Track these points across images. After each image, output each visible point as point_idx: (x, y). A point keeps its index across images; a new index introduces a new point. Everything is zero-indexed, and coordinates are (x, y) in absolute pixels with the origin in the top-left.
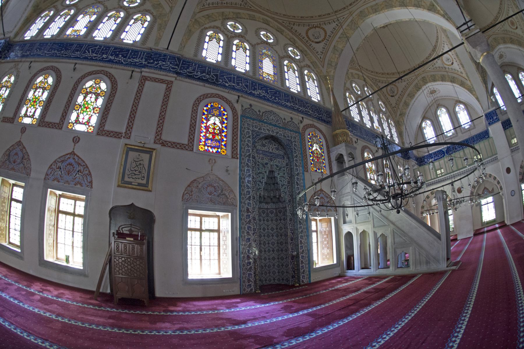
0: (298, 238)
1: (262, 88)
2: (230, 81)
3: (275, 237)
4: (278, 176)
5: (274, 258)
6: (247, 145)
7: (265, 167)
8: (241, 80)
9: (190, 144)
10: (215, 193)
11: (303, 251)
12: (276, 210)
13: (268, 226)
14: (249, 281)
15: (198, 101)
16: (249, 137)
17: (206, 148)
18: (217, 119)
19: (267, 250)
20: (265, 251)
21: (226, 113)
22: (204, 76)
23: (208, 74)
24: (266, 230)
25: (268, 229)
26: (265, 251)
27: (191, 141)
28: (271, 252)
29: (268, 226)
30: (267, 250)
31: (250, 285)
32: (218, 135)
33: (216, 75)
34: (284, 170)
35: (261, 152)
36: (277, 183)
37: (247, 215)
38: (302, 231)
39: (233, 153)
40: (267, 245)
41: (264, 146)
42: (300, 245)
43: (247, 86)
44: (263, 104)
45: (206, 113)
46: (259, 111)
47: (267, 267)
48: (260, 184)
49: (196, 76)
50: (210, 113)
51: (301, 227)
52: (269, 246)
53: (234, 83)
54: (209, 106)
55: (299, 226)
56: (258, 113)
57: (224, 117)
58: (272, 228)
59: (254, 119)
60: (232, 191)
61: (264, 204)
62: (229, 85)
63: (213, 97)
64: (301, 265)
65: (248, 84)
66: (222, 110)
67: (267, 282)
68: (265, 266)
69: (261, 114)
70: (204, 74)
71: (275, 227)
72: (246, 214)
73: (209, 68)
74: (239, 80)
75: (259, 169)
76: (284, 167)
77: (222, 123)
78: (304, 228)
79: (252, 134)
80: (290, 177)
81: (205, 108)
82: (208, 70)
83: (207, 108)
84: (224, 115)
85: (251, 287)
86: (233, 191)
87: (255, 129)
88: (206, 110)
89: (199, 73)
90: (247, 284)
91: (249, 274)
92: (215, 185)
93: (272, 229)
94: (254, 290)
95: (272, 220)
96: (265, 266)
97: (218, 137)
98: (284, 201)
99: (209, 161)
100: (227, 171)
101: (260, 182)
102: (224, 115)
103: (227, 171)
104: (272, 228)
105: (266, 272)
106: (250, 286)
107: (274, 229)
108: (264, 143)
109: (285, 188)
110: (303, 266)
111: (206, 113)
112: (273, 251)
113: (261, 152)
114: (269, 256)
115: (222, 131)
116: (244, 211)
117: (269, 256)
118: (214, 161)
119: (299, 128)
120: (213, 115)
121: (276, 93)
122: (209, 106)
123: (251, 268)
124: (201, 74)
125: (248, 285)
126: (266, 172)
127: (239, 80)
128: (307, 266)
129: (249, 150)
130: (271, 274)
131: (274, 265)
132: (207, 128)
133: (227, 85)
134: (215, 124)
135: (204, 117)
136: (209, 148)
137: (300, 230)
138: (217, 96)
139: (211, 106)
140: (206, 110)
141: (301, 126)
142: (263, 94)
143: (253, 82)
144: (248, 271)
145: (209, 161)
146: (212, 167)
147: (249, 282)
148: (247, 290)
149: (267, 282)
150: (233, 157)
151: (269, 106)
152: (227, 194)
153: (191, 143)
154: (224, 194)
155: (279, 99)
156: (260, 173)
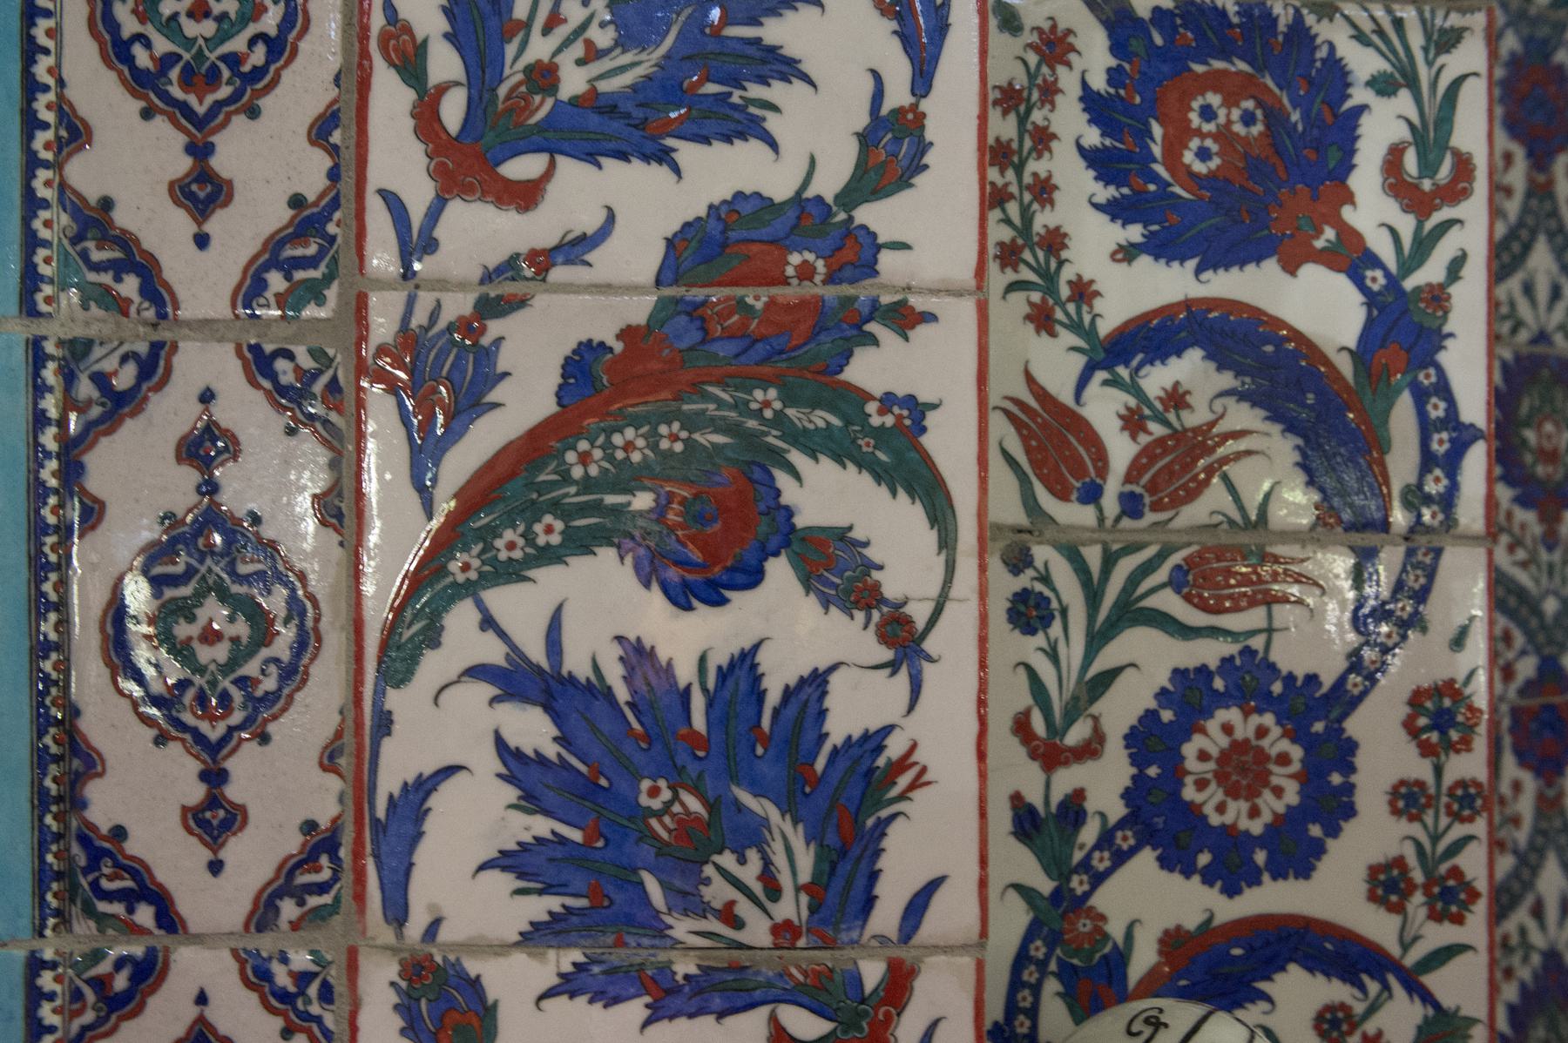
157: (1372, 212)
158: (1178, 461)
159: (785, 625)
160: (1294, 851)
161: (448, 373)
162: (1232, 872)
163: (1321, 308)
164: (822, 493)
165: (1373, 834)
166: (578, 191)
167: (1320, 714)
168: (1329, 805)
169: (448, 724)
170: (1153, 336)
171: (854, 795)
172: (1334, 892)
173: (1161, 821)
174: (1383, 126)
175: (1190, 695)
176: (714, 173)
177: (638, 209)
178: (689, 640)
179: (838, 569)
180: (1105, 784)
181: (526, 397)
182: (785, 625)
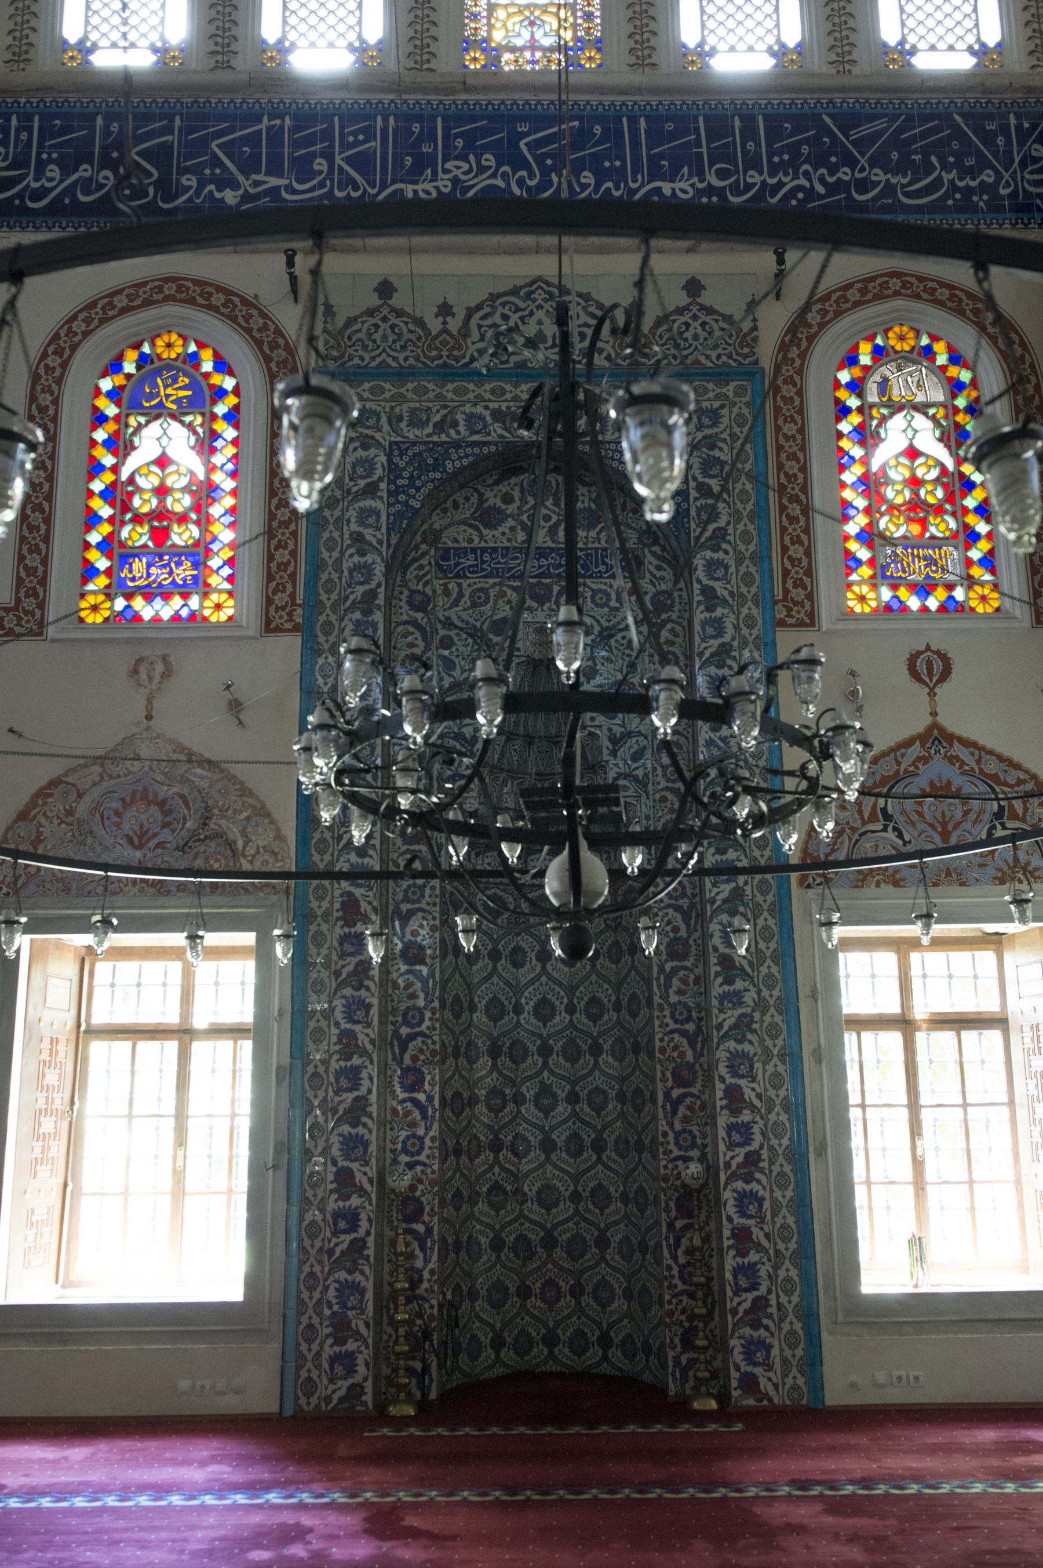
0: (713, 1065)
1: (470, 138)
2: (249, 166)
3: (606, 1058)
5: (600, 1196)
6: (358, 538)
8: (327, 135)
9: (29, 603)
10: (166, 835)
11: (752, 1160)
13: (571, 990)
14: (341, 1329)
15: (59, 352)
16: (371, 490)
17: (120, 604)
18: (176, 429)
19: (560, 1137)
20: (548, 1146)
21: (229, 383)
22: (86, 185)
23: (106, 163)
24: (562, 1018)
25: (571, 1009)
26: (548, 1146)
27: (30, 582)
28: (590, 1155)
29: (571, 990)
30: (560, 1137)
31: (351, 1356)
32: (183, 519)
33: (160, 156)
35: (470, 561)
37: (342, 940)
38: (744, 1024)
39: (269, 601)
40: (562, 1110)
42: (723, 1120)
43: (362, 163)
44: (471, 251)
45: (111, 410)
46: (445, 310)
47: (558, 1253)
49: (38, 195)
50: (135, 406)
51: (736, 1000)
52: (575, 1115)
53: (275, 169)
54: (129, 367)
55: (717, 989)
56: (435, 325)
57: (221, 409)
58: (594, 1001)
59: (401, 375)
60: (263, 812)
62: (246, 197)
63: (148, 303)
64: (730, 1261)
65: (376, 144)
66: (207, 366)
67: (563, 1352)
68: (549, 1242)
69: (454, 325)
70: (85, 171)
71: (606, 994)
72: (338, 931)
73: (109, 118)
74: (310, 140)
77: (207, 445)
78: (762, 1005)
79: (392, 468)
81: (106, 384)
82: (107, 132)
83: (119, 380)
84: (220, 393)
85: (351, 1371)
86: (268, 814)
87: (412, 434)
88: (114, 395)
89: (53, 171)
90: (328, 1351)
91: (347, 1289)
92: (164, 791)
93: (595, 1009)
94: (368, 1398)
96: (549, 1242)
97: (181, 536)
99: (135, 672)
100: (235, 706)
102: (220, 393)
103: (235, 706)
104: (594, 1001)
105: (550, 1283)
106: (347, 1361)
107: (603, 1010)
108: (493, 499)
109: (637, 756)
110: (750, 1271)
111: (111, 410)
112: (599, 1147)
113: (470, 561)
114: (576, 1179)
115: (204, 493)
116: (326, 915)
117: (576, 1179)
118: (160, 668)
119: (750, 339)
120: (156, 413)
121: (580, 139)
122: (129, 367)
123: (357, 1247)
124: (66, 172)
125: (333, 1360)
127: (310, 140)
128: (789, 1270)
129: (367, 570)
130: (587, 1300)
131: (602, 1242)
132: (119, 495)
133: (230, 197)
134: (162, 462)
135: (100, 435)
136: (138, 603)
137: (730, 1017)
138: (170, 289)
139: (143, 360)
140: (114, 395)
141: (774, 321)
142: (482, 182)
143: (407, 118)
144: (336, 1266)
145: (135, 672)
146: (150, 700)
147: (340, 1341)
148: (324, 1387)
149: (563, 1352)
150: (270, 628)
151: (521, 251)
152: (234, 832)
153: (33, 593)
154: (219, 835)
155: (601, 175)
157: (427, 1087)
158: (408, 1113)
159: (361, 1130)
160: (419, 1153)
161: (334, 1111)
162: (412, 1155)
163: (422, 1097)
164: (364, 1119)
165: (427, 1151)
166: (345, 1095)
167: (421, 1139)
168: (422, 1149)
169: (334, 1139)
170: (404, 1101)
171: (366, 1144)
172: (422, 1158)
173: (405, 1150)
174: (428, 1078)
175: (408, 1137)
176: (356, 1093)
177: (350, 1097)
178: (354, 1131)
179: (365, 1125)
180: (399, 1146)
181: (341, 1112)
182: (361, 1130)
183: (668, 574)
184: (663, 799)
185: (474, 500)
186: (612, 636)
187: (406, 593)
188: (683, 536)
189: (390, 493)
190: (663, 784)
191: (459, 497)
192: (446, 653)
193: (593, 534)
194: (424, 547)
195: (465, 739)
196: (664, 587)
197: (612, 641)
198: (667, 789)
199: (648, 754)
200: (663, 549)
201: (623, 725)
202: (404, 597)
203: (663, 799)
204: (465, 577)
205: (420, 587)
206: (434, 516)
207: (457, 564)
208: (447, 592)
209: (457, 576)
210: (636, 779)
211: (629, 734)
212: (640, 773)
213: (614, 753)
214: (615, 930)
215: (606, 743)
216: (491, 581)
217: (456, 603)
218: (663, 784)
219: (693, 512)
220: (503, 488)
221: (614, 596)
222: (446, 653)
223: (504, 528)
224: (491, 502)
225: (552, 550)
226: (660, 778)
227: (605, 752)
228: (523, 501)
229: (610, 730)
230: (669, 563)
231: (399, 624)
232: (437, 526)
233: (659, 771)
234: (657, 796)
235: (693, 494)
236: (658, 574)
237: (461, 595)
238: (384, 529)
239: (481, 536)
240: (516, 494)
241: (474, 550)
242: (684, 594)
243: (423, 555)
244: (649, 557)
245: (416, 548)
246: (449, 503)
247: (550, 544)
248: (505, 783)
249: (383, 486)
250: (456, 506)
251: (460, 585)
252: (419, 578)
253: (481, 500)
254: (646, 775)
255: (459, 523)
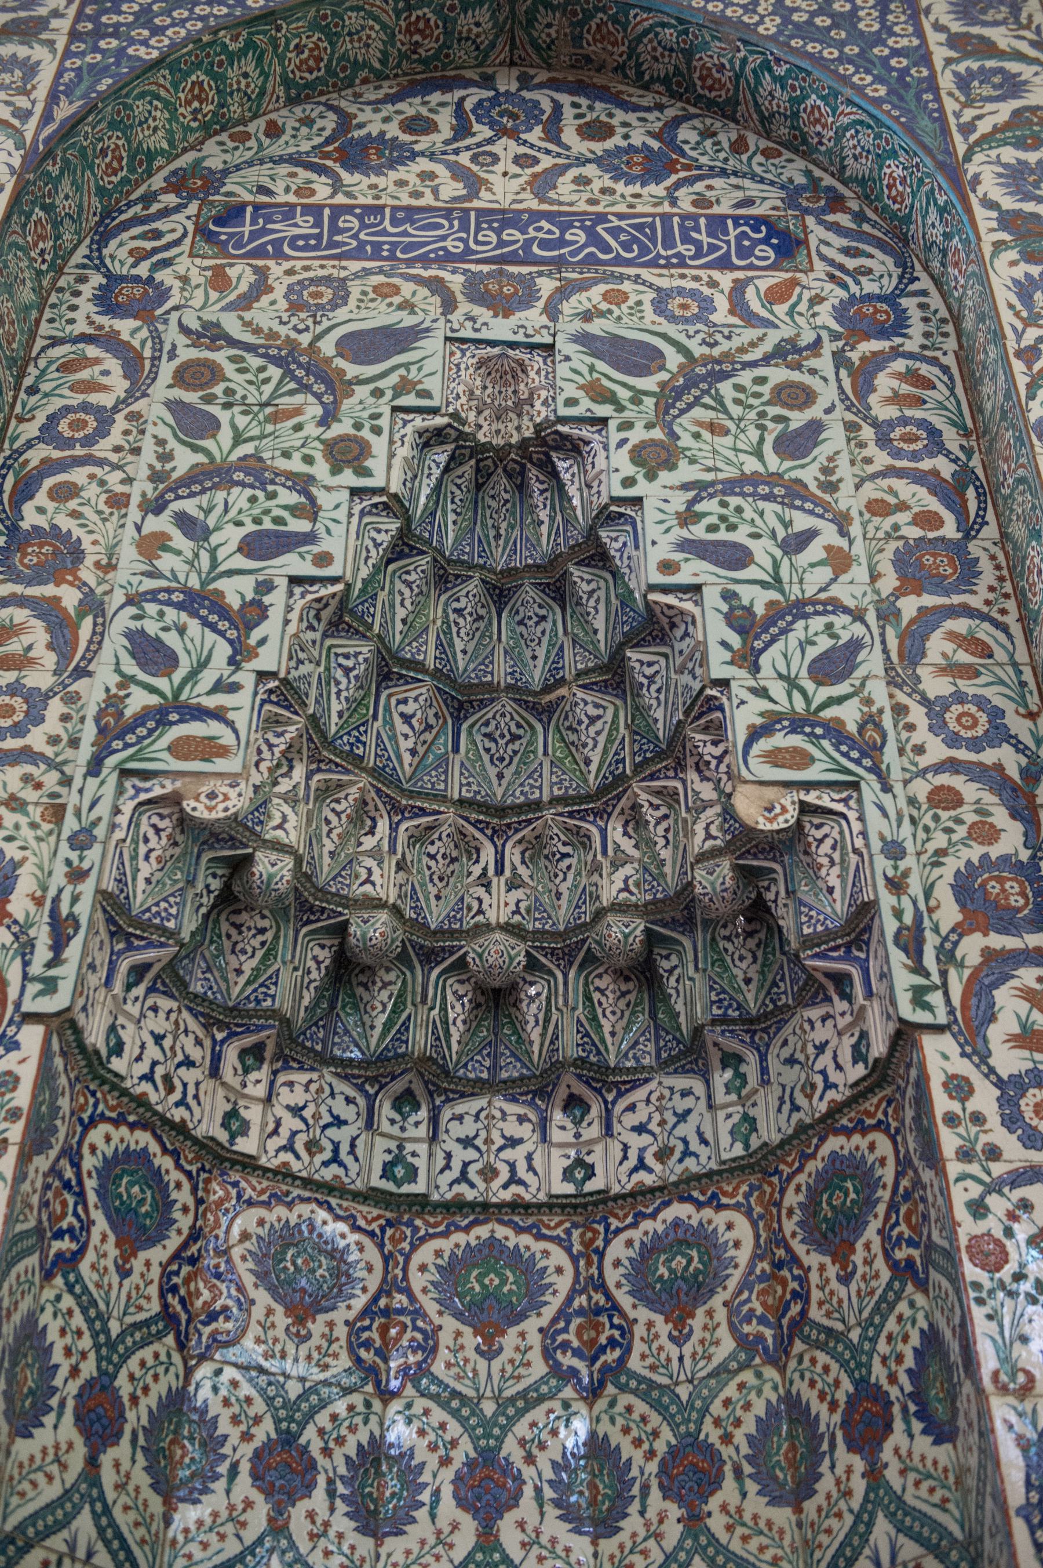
4: (660, 496)
7: (334, 388)
12: (767, 1217)
34: (798, 396)
36: (655, 627)
41: (356, 153)
48: (193, 639)
61: (511, 1117)
75: (194, 425)
76: (787, 352)
80: (951, 493)
95: (691, 1473)
98: (861, 921)
101: (203, 603)
109: (834, 666)
113: (304, 226)
126: (347, 454)
156: (213, 476)
183: (881, 263)
184: (946, 799)
185: (329, 123)
186: (724, 376)
187: (97, 279)
188: (924, 122)
189: (74, 35)
190: (937, 751)
191: (287, 118)
192: (192, 397)
193: (658, 190)
194: (171, 199)
195: (224, 612)
196: (870, 287)
197: (726, 388)
198: (952, 765)
199: (871, 662)
200: (860, 217)
201: (776, 583)
202: (87, 290)
203: (946, 799)
204: (279, 255)
205: (143, 270)
206: (210, 146)
207: (254, 235)
208: (219, 280)
209: (259, 253)
210: (835, 732)
211: (800, 609)
212: (850, 714)
213: (749, 659)
214: (778, 1358)
215: (715, 630)
216: (355, 266)
217: (246, 301)
218: (937, 751)
219: (946, 81)
220: (410, 107)
221: (722, 303)
222: (192, 397)
223: (410, 172)
224: (374, 129)
225: (536, 216)
226: (921, 734)
227: (718, 657)
228: (462, 130)
229: (728, 596)
230: (880, 245)
231: (55, 342)
232: (215, 163)
233: (917, 714)
234: (921, 789)
235: (940, 54)
236: (851, 263)
237: (262, 286)
238: (41, 93)
239: (337, 185)
240: (445, 120)
241: (314, 210)
242: (935, 301)
243: (165, 213)
244: (817, 232)
245: (148, 199)
246: (256, 127)
247: (534, 204)
248: (362, 817)
249: (64, 25)
250: (274, 131)
251: (262, 273)
252: (139, 256)
253: (345, 122)
254: (871, 720)
255: (280, 160)
